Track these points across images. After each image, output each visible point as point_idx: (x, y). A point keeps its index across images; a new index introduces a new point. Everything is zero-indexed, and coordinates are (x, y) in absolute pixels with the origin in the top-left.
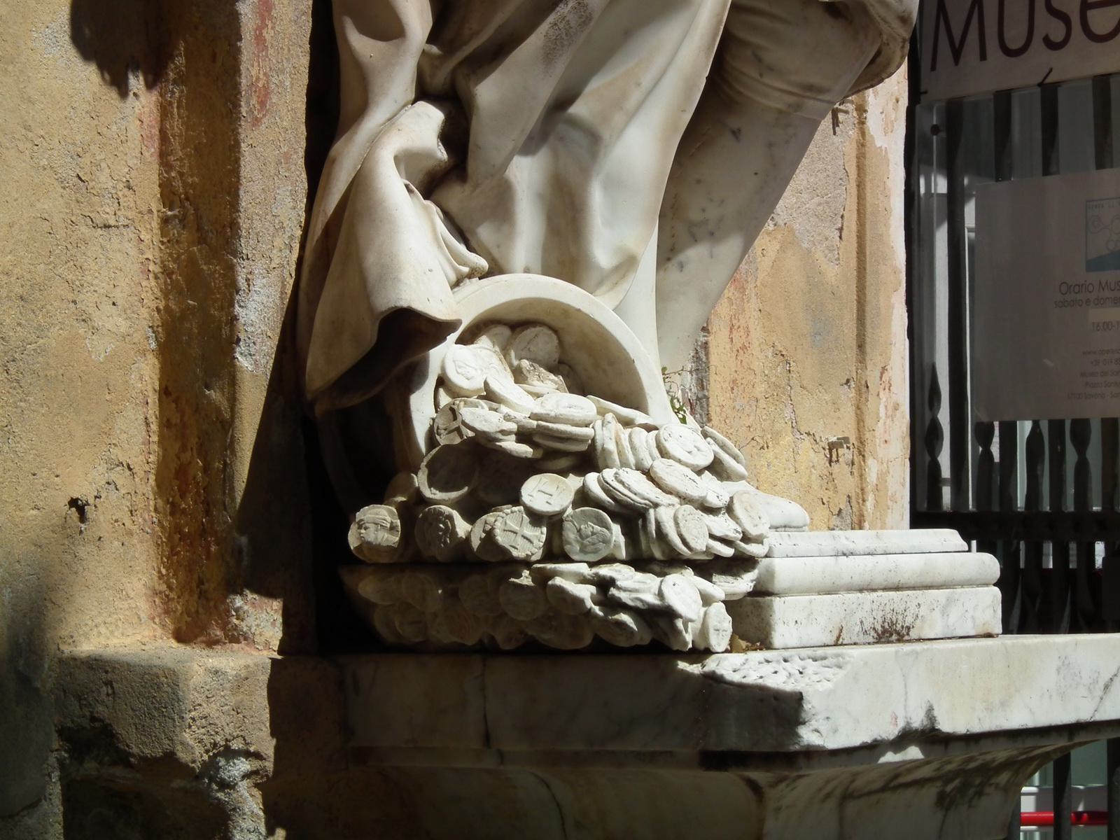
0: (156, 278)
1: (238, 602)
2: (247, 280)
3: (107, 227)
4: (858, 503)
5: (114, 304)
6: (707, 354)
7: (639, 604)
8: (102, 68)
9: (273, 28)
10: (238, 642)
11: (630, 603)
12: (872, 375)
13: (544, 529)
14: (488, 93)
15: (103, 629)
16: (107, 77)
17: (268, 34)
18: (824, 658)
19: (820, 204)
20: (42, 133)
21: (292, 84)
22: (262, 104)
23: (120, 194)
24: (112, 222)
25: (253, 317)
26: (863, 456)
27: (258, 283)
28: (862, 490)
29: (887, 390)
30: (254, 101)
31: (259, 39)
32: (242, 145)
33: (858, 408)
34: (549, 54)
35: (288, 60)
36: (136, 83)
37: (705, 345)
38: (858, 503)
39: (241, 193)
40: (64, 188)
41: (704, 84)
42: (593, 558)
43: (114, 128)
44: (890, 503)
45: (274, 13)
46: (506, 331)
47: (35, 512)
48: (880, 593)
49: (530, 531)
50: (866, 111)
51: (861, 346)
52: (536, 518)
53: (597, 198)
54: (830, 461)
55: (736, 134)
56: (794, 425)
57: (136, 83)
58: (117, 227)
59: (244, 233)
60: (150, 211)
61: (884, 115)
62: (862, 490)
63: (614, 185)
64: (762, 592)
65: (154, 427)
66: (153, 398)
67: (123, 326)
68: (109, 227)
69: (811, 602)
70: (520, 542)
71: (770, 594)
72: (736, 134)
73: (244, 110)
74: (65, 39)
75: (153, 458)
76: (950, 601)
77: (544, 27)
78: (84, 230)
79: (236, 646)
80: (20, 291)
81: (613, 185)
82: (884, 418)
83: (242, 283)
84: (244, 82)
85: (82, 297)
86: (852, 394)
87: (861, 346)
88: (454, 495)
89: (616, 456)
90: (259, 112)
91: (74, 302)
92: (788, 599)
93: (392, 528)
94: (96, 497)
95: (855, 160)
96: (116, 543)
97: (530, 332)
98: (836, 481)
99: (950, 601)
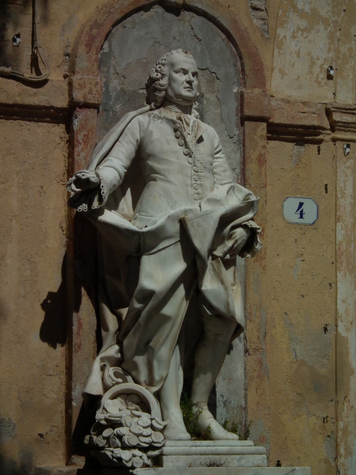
0: (65, 386)
1: (73, 456)
2: (75, 386)
3: (51, 375)
4: (336, 434)
5: (53, 392)
6: (247, 396)
7: (116, 457)
8: (48, 343)
9: (82, 331)
10: (73, 465)
11: (115, 456)
12: (340, 398)
13: (106, 440)
14: (125, 342)
15: (49, 462)
16: (50, 345)
17: (81, 332)
18: (155, 469)
19: (318, 353)
20: (32, 357)
21: (88, 342)
22: (79, 348)
23: (54, 368)
24: (52, 374)
25: (76, 394)
26: (337, 421)
27: (78, 387)
28: (337, 430)
29: (348, 402)
30: (76, 347)
31: (78, 333)
32: (73, 357)
33: (336, 408)
34: (134, 334)
35: (87, 337)
36: (58, 345)
37: (246, 394)
38: (336, 434)
39: (73, 367)
40: (39, 368)
41: (177, 338)
42: (114, 447)
43: (53, 354)
44: (349, 434)
45: (83, 327)
46: (126, 396)
47: (29, 437)
48: (210, 456)
49: (103, 441)
50: (338, 327)
51: (336, 391)
52: (104, 438)
53: (155, 364)
54: (324, 422)
55: (205, 346)
56: (307, 412)
57: (58, 345)
58: (54, 375)
59: (73, 376)
60: (63, 371)
61: (346, 327)
62: (337, 430)
63: (159, 361)
64: (162, 455)
65: (64, 418)
66: (64, 412)
67: (55, 396)
68: (51, 375)
69: (178, 457)
70: (101, 443)
71: (164, 455)
72: (205, 346)
73: (73, 350)
74: (38, 337)
75: (64, 425)
76: (241, 458)
77: (134, 328)
78: (44, 376)
79: (72, 466)
80: (26, 390)
81: (159, 361)
82: (346, 410)
83: (73, 387)
84: (74, 343)
85: (43, 391)
86: (334, 404)
87: (336, 391)
88: (95, 433)
89: (124, 424)
90: (78, 349)
91: (41, 392)
92: (168, 456)
93: (88, 440)
94: (46, 433)
95: (335, 340)
96: (54, 443)
97: (131, 396)
98: (326, 428)
99: (241, 458)
